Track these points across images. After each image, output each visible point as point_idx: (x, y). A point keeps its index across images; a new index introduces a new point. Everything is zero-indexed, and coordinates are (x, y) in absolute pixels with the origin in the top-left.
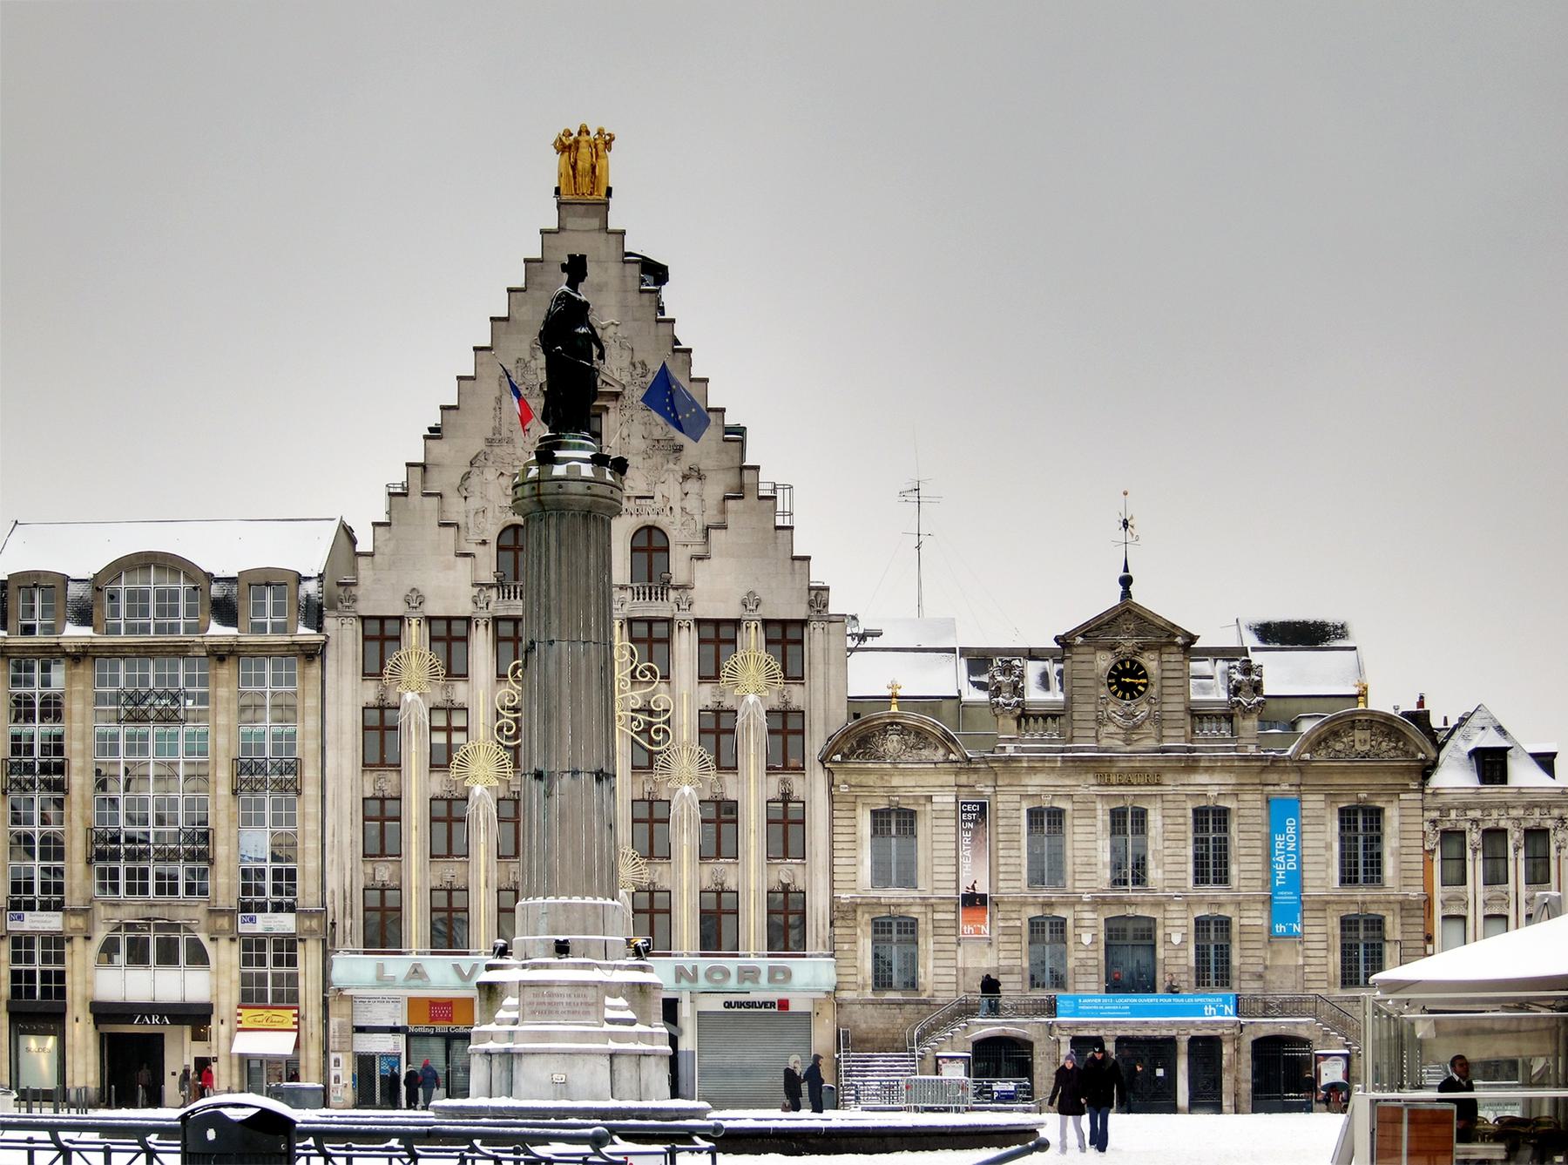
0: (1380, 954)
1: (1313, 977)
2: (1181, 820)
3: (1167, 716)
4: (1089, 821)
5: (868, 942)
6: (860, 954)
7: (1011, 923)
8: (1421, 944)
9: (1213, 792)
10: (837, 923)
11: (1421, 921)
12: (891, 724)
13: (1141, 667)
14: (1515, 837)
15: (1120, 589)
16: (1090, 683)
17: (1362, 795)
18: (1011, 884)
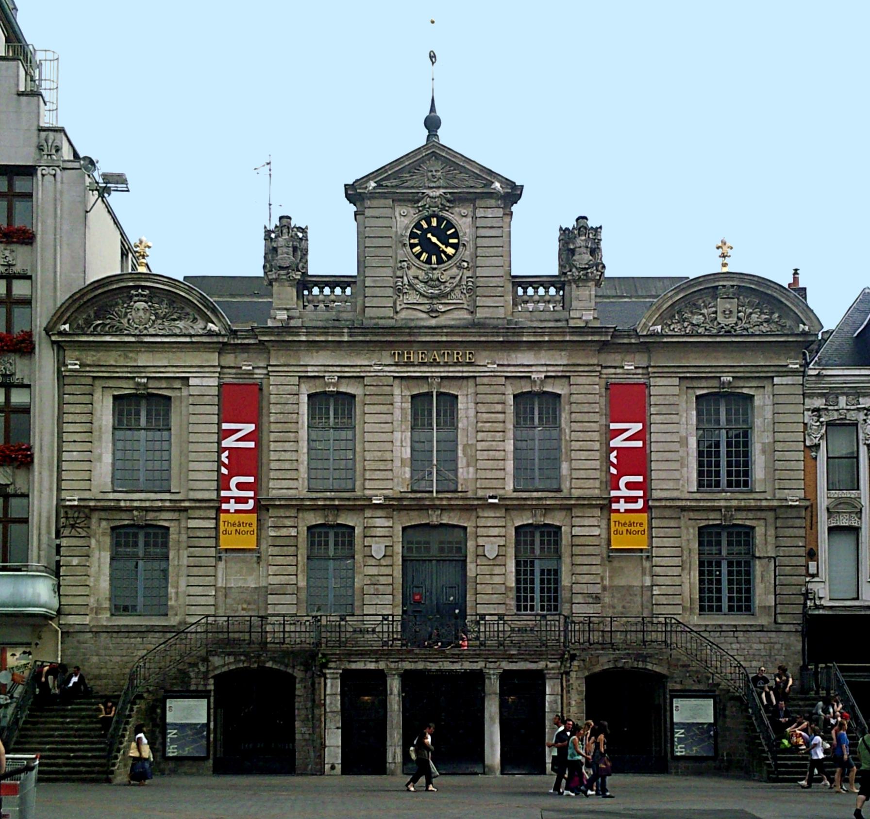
1: (663, 600)
2: (499, 408)
3: (481, 282)
4: (384, 408)
5: (106, 556)
6: (93, 571)
7: (284, 532)
8: (802, 561)
18: (285, 484)
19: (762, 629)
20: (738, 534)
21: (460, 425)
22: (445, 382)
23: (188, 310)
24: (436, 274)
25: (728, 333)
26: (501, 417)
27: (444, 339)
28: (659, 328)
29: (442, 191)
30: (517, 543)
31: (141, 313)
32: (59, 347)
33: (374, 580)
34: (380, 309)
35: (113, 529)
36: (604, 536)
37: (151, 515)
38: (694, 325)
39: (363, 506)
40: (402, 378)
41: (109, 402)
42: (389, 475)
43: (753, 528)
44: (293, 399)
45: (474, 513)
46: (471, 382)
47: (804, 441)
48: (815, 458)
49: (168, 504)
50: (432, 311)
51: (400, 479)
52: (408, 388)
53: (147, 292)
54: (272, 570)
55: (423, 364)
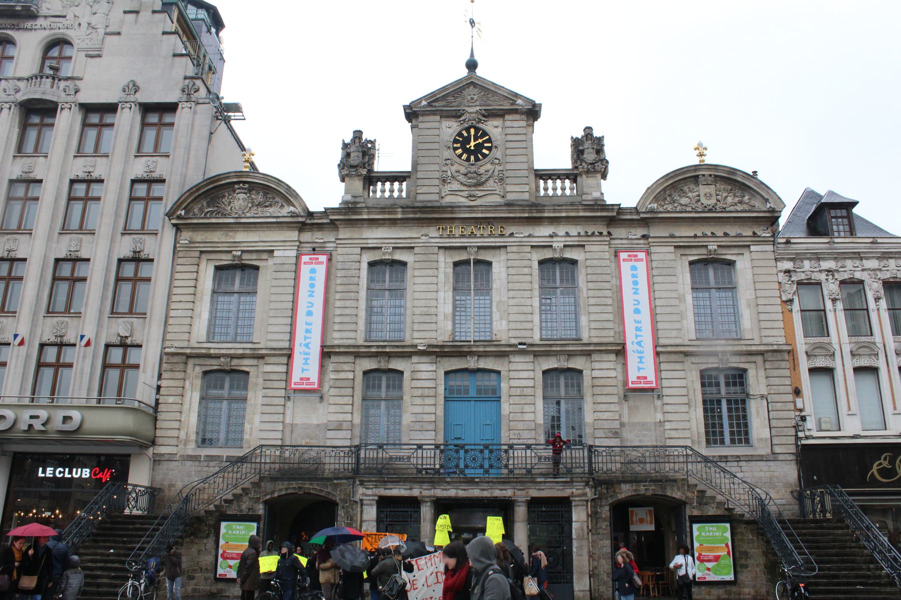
0: (744, 410)
1: (674, 434)
2: (526, 271)
3: (508, 174)
4: (430, 272)
5: (196, 396)
6: (186, 407)
7: (342, 375)
8: (790, 397)
9: (558, 244)
10: (165, 375)
11: (787, 373)
12: (238, 183)
13: (485, 134)
14: (873, 288)
15: (467, 71)
16: (436, 146)
17: (713, 247)
18: (345, 335)
19: (761, 458)
21: (494, 286)
22: (482, 252)
23: (277, 199)
24: (473, 169)
25: (710, 211)
26: (528, 278)
27: (480, 215)
29: (478, 108)
30: (545, 387)
31: (241, 202)
32: (178, 228)
33: (419, 417)
34: (428, 194)
36: (620, 378)
37: (235, 362)
40: (446, 248)
41: (211, 270)
42: (434, 326)
43: (745, 370)
44: (356, 265)
45: (506, 360)
46: (503, 250)
47: (780, 297)
48: (791, 311)
49: (248, 352)
51: (442, 331)
52: (451, 257)
53: (247, 186)
54: (332, 409)
55: (462, 236)
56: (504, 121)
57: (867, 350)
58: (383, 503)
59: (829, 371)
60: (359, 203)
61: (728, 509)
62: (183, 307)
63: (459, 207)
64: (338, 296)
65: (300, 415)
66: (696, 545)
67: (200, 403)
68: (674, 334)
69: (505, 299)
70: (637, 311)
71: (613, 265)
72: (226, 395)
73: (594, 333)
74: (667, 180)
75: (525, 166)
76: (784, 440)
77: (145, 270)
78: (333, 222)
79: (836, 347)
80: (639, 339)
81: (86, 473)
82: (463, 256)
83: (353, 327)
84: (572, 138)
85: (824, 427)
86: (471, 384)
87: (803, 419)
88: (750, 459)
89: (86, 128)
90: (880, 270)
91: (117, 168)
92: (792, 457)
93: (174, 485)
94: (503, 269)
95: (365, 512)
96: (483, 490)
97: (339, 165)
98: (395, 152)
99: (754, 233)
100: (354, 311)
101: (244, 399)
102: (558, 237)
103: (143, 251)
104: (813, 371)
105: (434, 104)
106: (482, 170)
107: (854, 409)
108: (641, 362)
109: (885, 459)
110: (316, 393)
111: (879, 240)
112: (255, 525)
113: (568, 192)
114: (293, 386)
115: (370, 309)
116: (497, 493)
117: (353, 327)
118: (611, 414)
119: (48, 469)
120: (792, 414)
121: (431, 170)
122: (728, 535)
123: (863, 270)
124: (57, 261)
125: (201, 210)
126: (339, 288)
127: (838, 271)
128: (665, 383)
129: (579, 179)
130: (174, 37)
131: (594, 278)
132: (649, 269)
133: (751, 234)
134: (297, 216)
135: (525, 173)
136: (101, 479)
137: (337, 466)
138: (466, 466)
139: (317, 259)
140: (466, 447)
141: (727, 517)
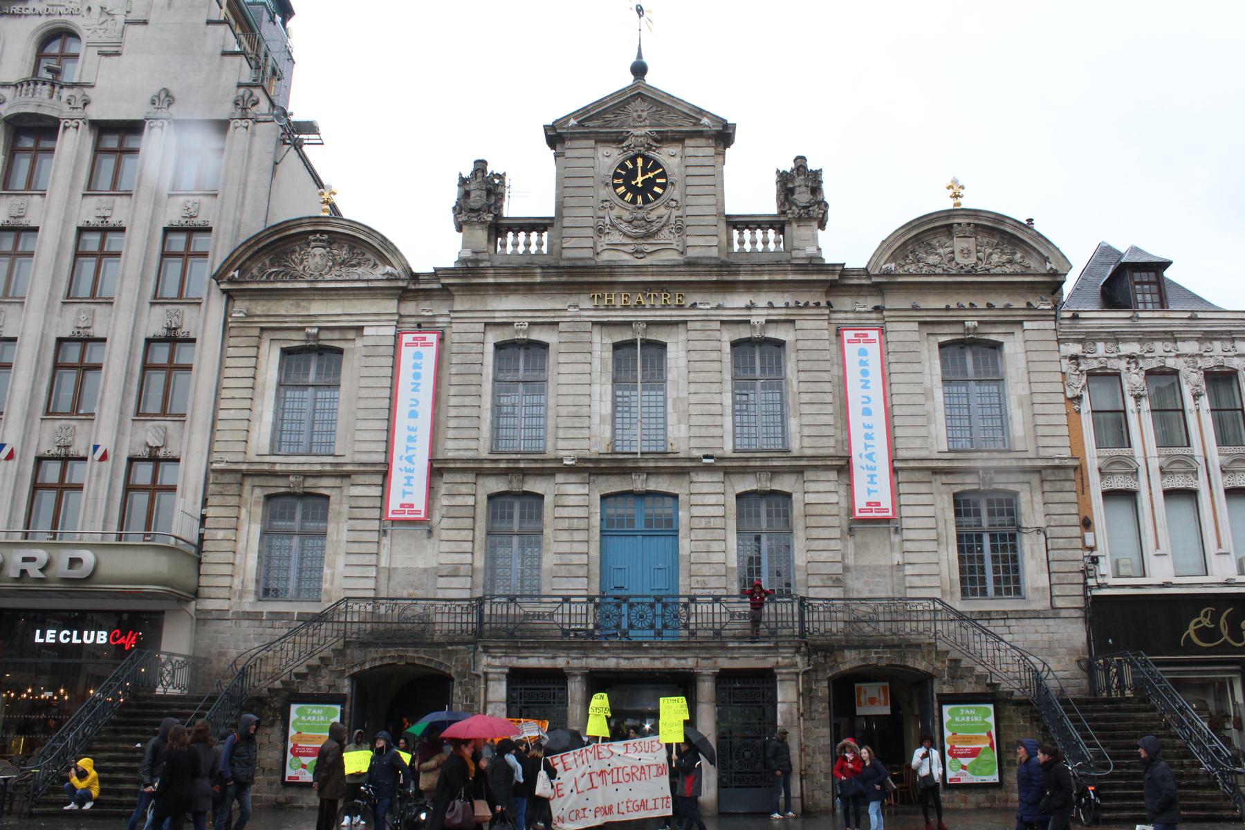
0: (1014, 548)
1: (917, 581)
2: (714, 355)
4: (580, 357)
5: (256, 530)
6: (241, 545)
7: (459, 501)
8: (1077, 531)
9: (758, 318)
10: (212, 501)
11: (1072, 497)
13: (657, 165)
14: (1192, 380)
15: (632, 78)
18: (463, 444)
19: (1037, 615)
20: (1000, 502)
21: (670, 377)
23: (368, 256)
24: (641, 214)
25: (968, 273)
26: (716, 366)
27: (650, 279)
28: (893, 266)
30: (740, 516)
31: (318, 259)
32: (229, 296)
33: (566, 559)
34: (578, 248)
35: (269, 497)
36: (844, 504)
37: (310, 482)
38: (929, 265)
39: (551, 469)
40: (602, 324)
41: (275, 355)
42: (586, 433)
43: (1016, 494)
44: (478, 348)
45: (687, 478)
46: (681, 328)
47: (1064, 393)
48: (1079, 412)
49: (328, 468)
50: (637, 252)
51: (597, 439)
52: (610, 336)
54: (445, 547)
55: (626, 307)
56: (684, 147)
57: (1183, 466)
58: (516, 677)
59: (1130, 495)
60: (483, 261)
61: (992, 685)
62: (238, 405)
63: (622, 267)
64: (453, 390)
65: (400, 555)
66: (947, 734)
67: (261, 539)
68: (918, 443)
69: (685, 394)
70: (866, 412)
71: (834, 348)
72: (297, 528)
73: (807, 442)
74: (909, 231)
75: (712, 210)
76: (1068, 590)
77: (184, 355)
78: (445, 287)
79: (1141, 461)
80: (870, 450)
81: (102, 637)
82: (627, 336)
83: (474, 433)
84: (778, 171)
85: (1123, 571)
86: (638, 513)
87: (1095, 560)
88: (1021, 615)
89: (100, 156)
90: (1201, 356)
91: (144, 212)
92: (1079, 613)
93: (224, 654)
94: (683, 354)
95: (490, 689)
96: (654, 659)
97: (454, 209)
98: (532, 190)
99: (1029, 304)
100: (475, 412)
101: (323, 534)
102: (759, 309)
103: (180, 327)
104: (1108, 495)
105: (587, 124)
106: (653, 216)
107: (1164, 547)
108: (872, 482)
109: (1206, 616)
110: (423, 525)
111: (1200, 315)
112: (338, 708)
113: (772, 247)
114: (390, 516)
115: (497, 408)
116: (673, 663)
117: (474, 433)
118: (831, 554)
119: (49, 632)
120: (1079, 554)
121: (582, 216)
122: (991, 720)
123: (1177, 356)
124: (60, 341)
125: (262, 271)
126: (454, 380)
127: (1143, 357)
128: (905, 511)
129: (787, 229)
130: (223, 28)
131: (807, 365)
132: (884, 353)
133: (1024, 305)
134: (397, 279)
135: (713, 220)
136: (123, 645)
137: (452, 627)
138: (631, 627)
139: (424, 339)
140: (631, 600)
141: (990, 695)
